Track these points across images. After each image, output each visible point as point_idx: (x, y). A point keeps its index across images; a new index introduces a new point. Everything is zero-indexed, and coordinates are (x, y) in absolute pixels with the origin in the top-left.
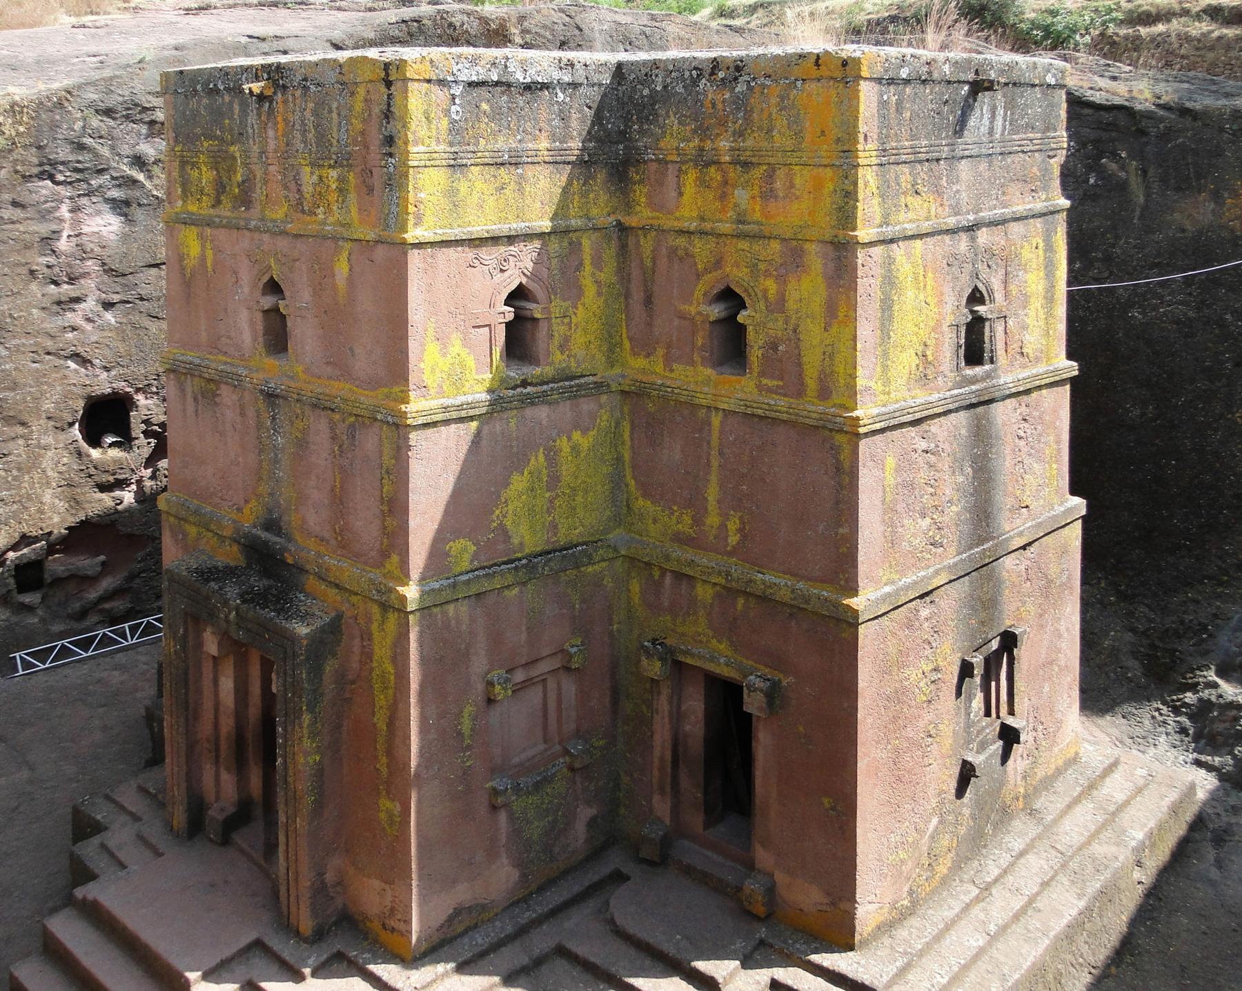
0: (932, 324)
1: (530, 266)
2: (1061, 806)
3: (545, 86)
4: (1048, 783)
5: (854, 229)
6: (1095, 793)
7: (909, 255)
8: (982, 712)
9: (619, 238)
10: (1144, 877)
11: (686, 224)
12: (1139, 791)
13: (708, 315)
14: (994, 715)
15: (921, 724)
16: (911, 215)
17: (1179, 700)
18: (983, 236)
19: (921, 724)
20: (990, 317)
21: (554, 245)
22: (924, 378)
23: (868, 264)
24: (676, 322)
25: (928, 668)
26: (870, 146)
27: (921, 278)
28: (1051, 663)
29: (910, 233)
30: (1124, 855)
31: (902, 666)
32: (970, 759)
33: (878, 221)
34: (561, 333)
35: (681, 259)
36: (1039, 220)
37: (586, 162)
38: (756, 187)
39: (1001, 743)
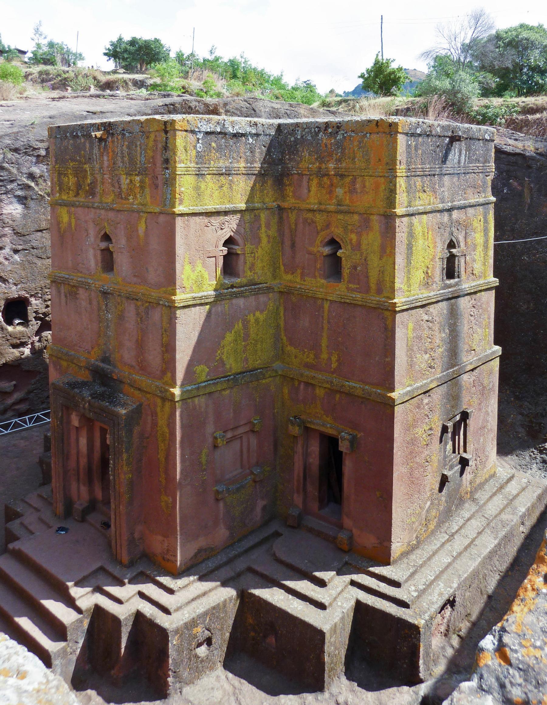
0: (431, 257)
1: (235, 227)
2: (487, 497)
3: (243, 135)
4: (481, 486)
5: (395, 208)
6: (503, 491)
7: (420, 222)
8: (451, 451)
9: (279, 214)
10: (524, 529)
11: (312, 206)
12: (523, 489)
13: (323, 253)
14: (457, 452)
15: (423, 456)
16: (421, 202)
17: (542, 447)
18: (455, 214)
19: (423, 456)
20: (458, 255)
21: (247, 217)
22: (427, 285)
23: (401, 225)
24: (307, 256)
25: (427, 428)
26: (402, 167)
27: (426, 234)
28: (484, 427)
29: (421, 211)
30: (516, 519)
31: (415, 426)
32: (446, 473)
33: (406, 205)
34: (250, 261)
35: (309, 224)
37: (263, 174)
38: (347, 188)
39: (460, 466)
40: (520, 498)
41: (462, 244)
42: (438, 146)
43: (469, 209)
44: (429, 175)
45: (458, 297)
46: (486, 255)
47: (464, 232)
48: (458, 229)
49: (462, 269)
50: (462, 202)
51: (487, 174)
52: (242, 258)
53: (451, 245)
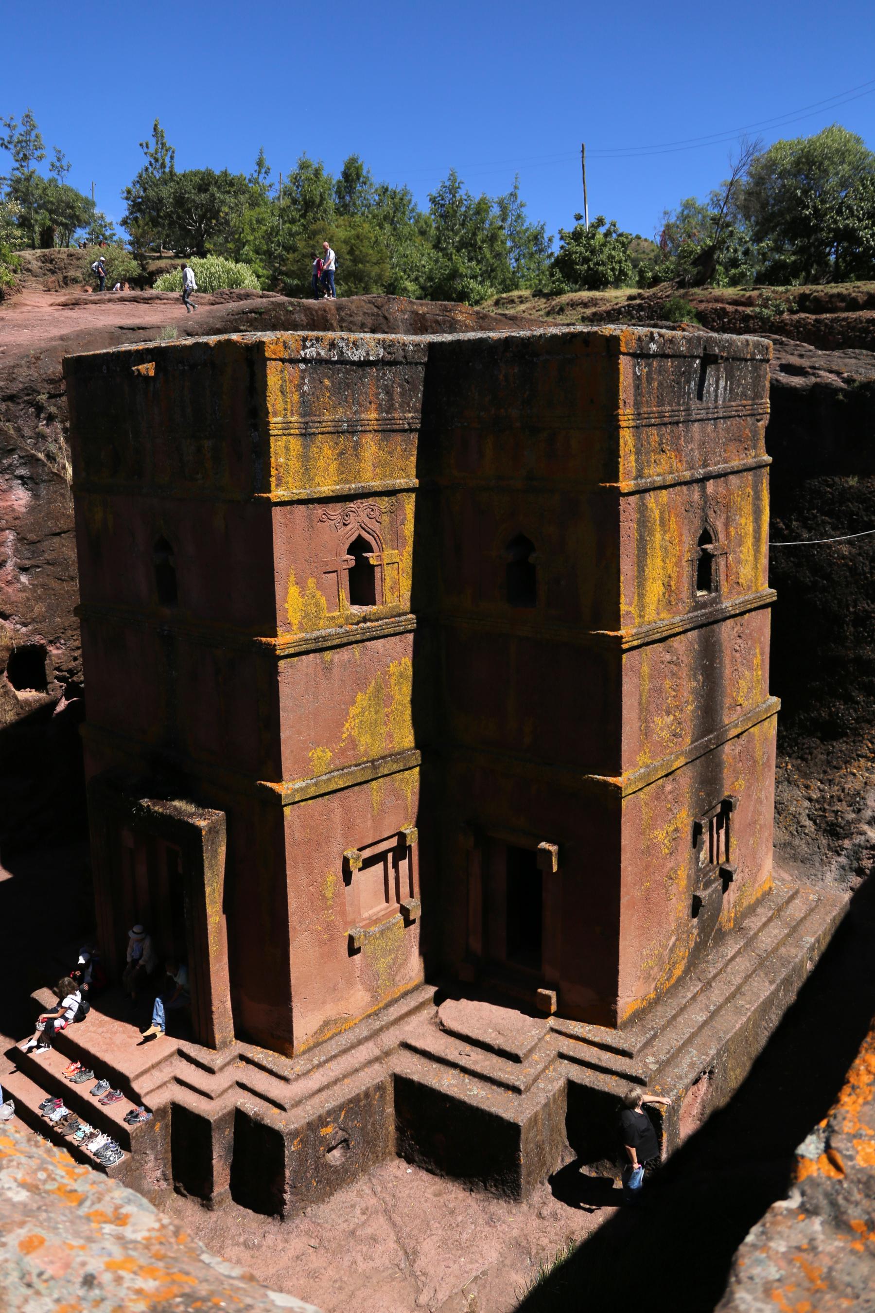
2: (760, 924)
4: (751, 910)
6: (782, 913)
12: (812, 910)
14: (715, 862)
15: (666, 870)
18: (710, 486)
31: (653, 828)
33: (634, 474)
36: (751, 473)
40: (807, 924)
41: (721, 536)
42: (684, 372)
43: (731, 477)
44: (670, 423)
45: (716, 622)
46: (757, 551)
47: (724, 516)
48: (715, 512)
49: (723, 577)
50: (721, 466)
51: (758, 417)
52: (377, 570)
53: (706, 537)
